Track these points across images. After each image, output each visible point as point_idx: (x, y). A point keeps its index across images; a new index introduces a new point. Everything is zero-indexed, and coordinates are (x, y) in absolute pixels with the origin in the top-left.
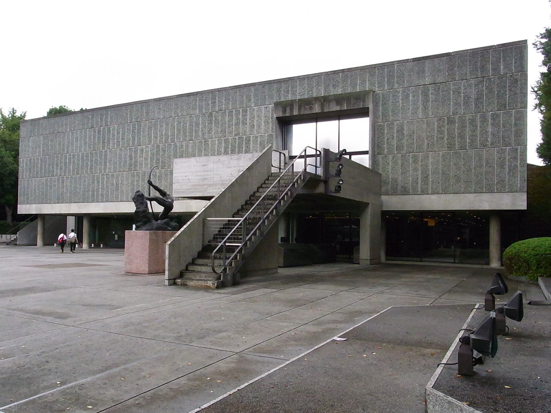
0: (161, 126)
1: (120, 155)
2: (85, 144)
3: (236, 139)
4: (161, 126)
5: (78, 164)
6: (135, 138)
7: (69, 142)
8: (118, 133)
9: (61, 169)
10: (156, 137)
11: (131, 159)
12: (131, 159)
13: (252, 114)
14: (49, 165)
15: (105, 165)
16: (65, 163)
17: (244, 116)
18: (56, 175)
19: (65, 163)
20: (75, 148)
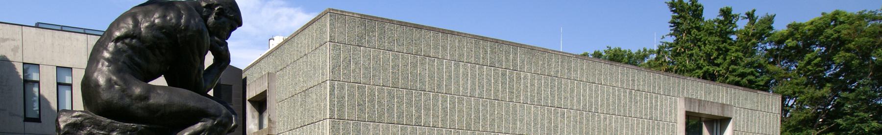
0: (585, 90)
1: (536, 115)
2: (481, 86)
3: (650, 122)
4: (585, 90)
5: (469, 115)
6: (555, 96)
7: (450, 77)
8: (533, 85)
9: (436, 116)
10: (579, 102)
11: (550, 122)
12: (550, 122)
13: (661, 102)
14: (409, 104)
15: (515, 124)
16: (444, 110)
17: (656, 101)
18: (424, 124)
19: (444, 110)
20: (461, 89)
